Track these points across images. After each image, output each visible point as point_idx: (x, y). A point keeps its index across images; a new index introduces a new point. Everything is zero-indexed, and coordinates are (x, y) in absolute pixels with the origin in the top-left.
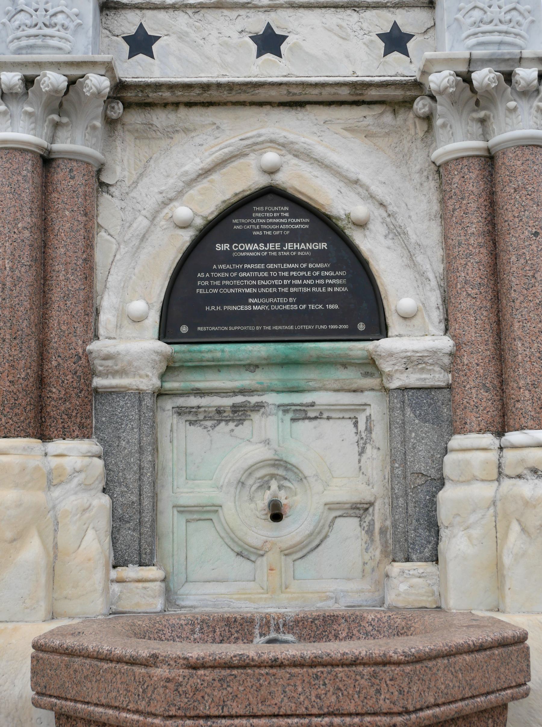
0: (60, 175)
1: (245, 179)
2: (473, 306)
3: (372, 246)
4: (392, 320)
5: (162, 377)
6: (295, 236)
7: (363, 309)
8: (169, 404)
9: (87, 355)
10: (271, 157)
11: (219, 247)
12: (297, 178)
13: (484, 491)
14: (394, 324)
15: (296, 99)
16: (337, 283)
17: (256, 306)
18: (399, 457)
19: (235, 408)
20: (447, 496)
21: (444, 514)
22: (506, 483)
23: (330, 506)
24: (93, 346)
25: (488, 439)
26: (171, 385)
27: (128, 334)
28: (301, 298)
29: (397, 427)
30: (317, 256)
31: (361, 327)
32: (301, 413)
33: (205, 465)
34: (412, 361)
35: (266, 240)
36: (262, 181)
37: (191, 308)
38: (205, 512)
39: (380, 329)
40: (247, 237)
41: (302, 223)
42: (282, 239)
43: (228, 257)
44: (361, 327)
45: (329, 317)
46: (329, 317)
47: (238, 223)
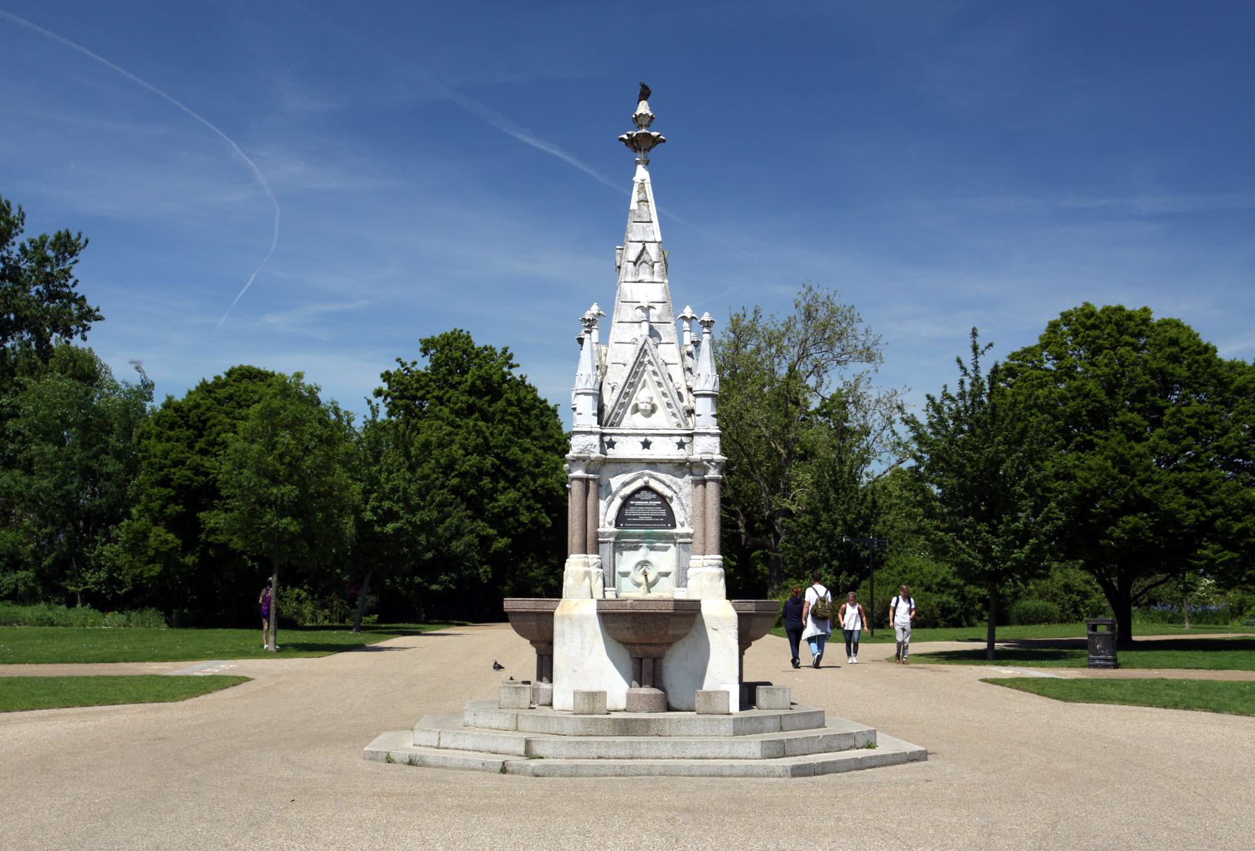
2: (698, 520)
6: (652, 500)
7: (670, 520)
10: (646, 478)
12: (654, 484)
14: (678, 525)
15: (652, 464)
16: (663, 513)
17: (642, 519)
18: (679, 560)
32: (652, 549)
33: (628, 561)
38: (625, 574)
39: (674, 526)
40: (639, 500)
41: (654, 496)
47: (637, 496)
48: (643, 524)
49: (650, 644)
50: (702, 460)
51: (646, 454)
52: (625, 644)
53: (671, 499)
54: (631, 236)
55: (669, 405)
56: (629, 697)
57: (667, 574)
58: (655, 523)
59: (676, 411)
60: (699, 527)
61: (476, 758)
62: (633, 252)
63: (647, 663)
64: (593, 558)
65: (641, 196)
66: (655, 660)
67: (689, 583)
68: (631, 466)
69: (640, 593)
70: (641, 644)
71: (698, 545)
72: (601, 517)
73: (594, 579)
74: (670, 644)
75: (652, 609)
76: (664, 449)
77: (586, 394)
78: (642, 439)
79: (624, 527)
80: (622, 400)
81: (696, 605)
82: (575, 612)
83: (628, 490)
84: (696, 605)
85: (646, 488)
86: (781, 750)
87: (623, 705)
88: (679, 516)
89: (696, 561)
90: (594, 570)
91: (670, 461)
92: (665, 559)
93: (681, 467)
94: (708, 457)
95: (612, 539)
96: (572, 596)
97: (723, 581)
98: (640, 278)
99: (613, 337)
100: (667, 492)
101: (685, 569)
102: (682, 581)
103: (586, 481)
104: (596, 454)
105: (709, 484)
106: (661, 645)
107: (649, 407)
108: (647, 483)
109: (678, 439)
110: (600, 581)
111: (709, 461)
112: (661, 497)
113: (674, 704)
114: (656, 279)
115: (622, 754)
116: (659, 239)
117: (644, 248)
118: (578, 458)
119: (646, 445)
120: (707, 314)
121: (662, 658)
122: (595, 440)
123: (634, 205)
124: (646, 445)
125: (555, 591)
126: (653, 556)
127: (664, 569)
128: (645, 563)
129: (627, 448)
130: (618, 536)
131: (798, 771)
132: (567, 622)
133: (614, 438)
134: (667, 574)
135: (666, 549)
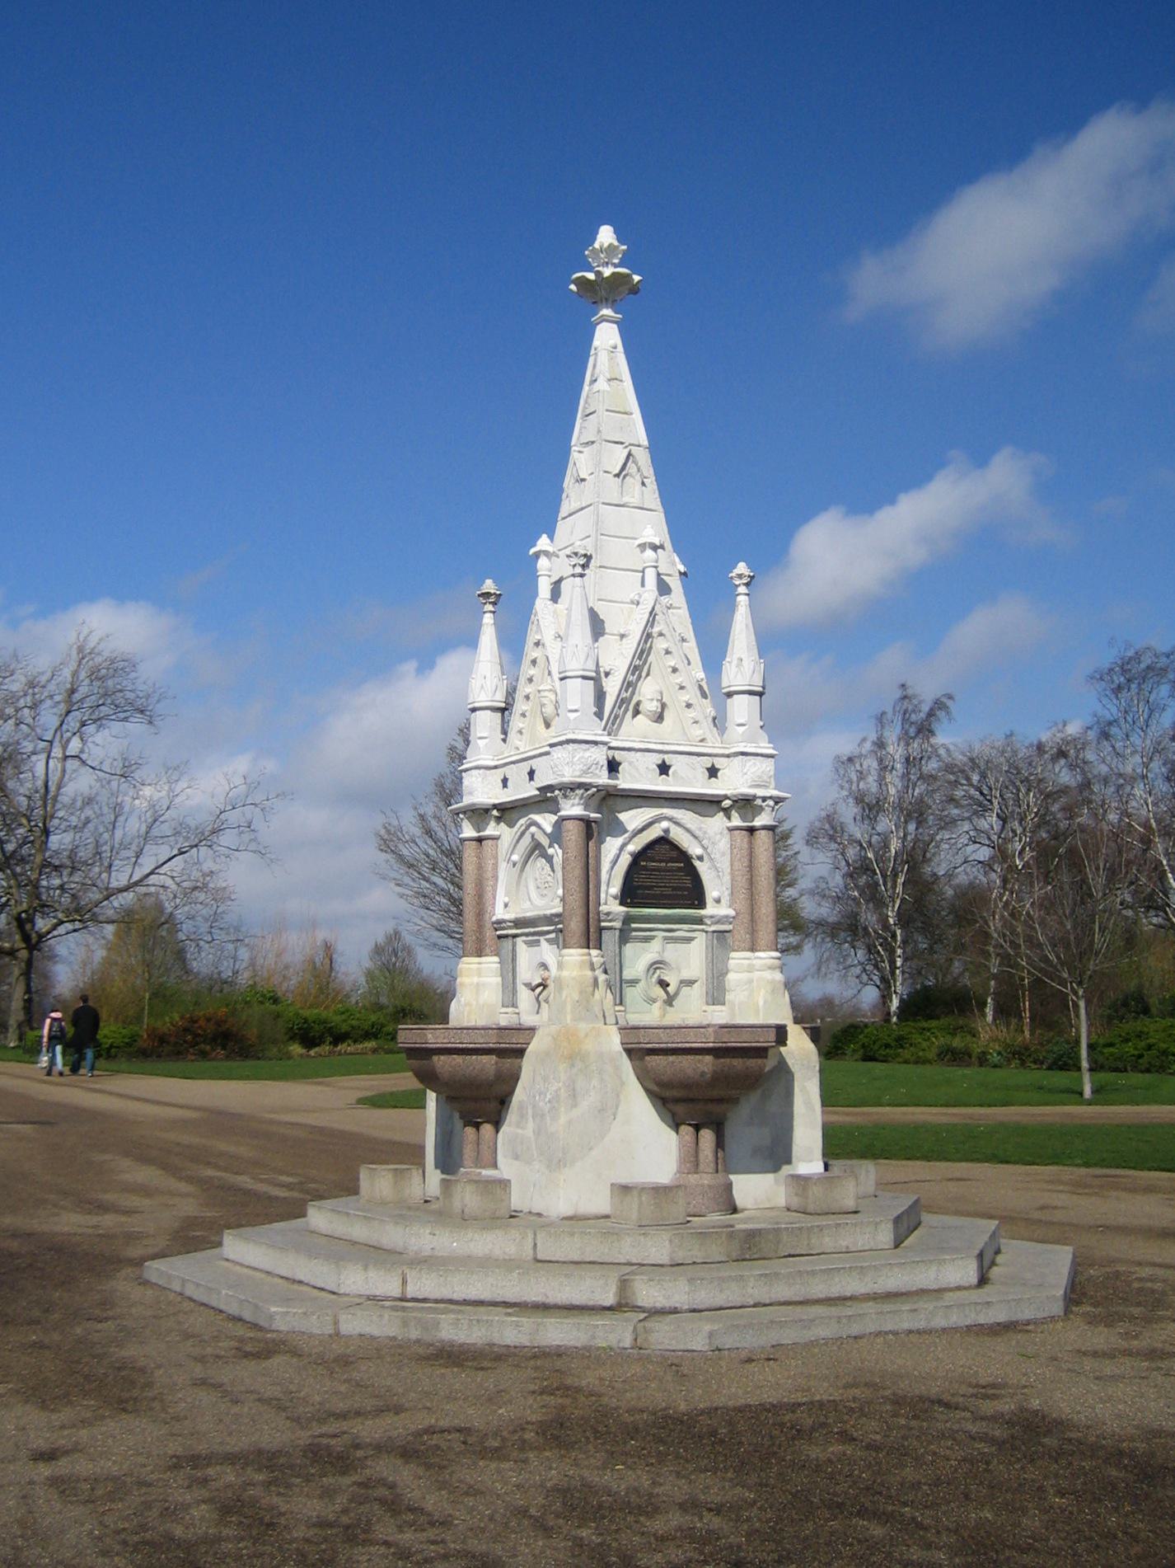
1: (654, 833)
2: (742, 895)
3: (702, 868)
6: (672, 860)
7: (695, 895)
10: (665, 824)
12: (677, 835)
13: (745, 976)
16: (688, 882)
17: (658, 891)
20: (731, 976)
23: (682, 982)
25: (748, 954)
27: (610, 904)
28: (674, 889)
29: (710, 948)
34: (720, 920)
35: (661, 861)
37: (630, 894)
39: (702, 904)
41: (674, 854)
43: (645, 868)
45: (683, 897)
46: (683, 897)
53: (700, 858)
57: (690, 983)
59: (700, 718)
60: (742, 905)
71: (741, 934)
72: (603, 887)
76: (688, 779)
77: (584, 678)
80: (624, 695)
88: (711, 893)
89: (738, 959)
93: (706, 804)
95: (618, 924)
98: (626, 499)
100: (694, 850)
101: (724, 973)
102: (716, 995)
103: (587, 823)
104: (603, 778)
105: (762, 835)
108: (667, 831)
109: (708, 762)
116: (646, 443)
126: (672, 953)
127: (686, 974)
128: (656, 965)
129: (637, 776)
130: (628, 919)
134: (690, 983)
135: (689, 940)
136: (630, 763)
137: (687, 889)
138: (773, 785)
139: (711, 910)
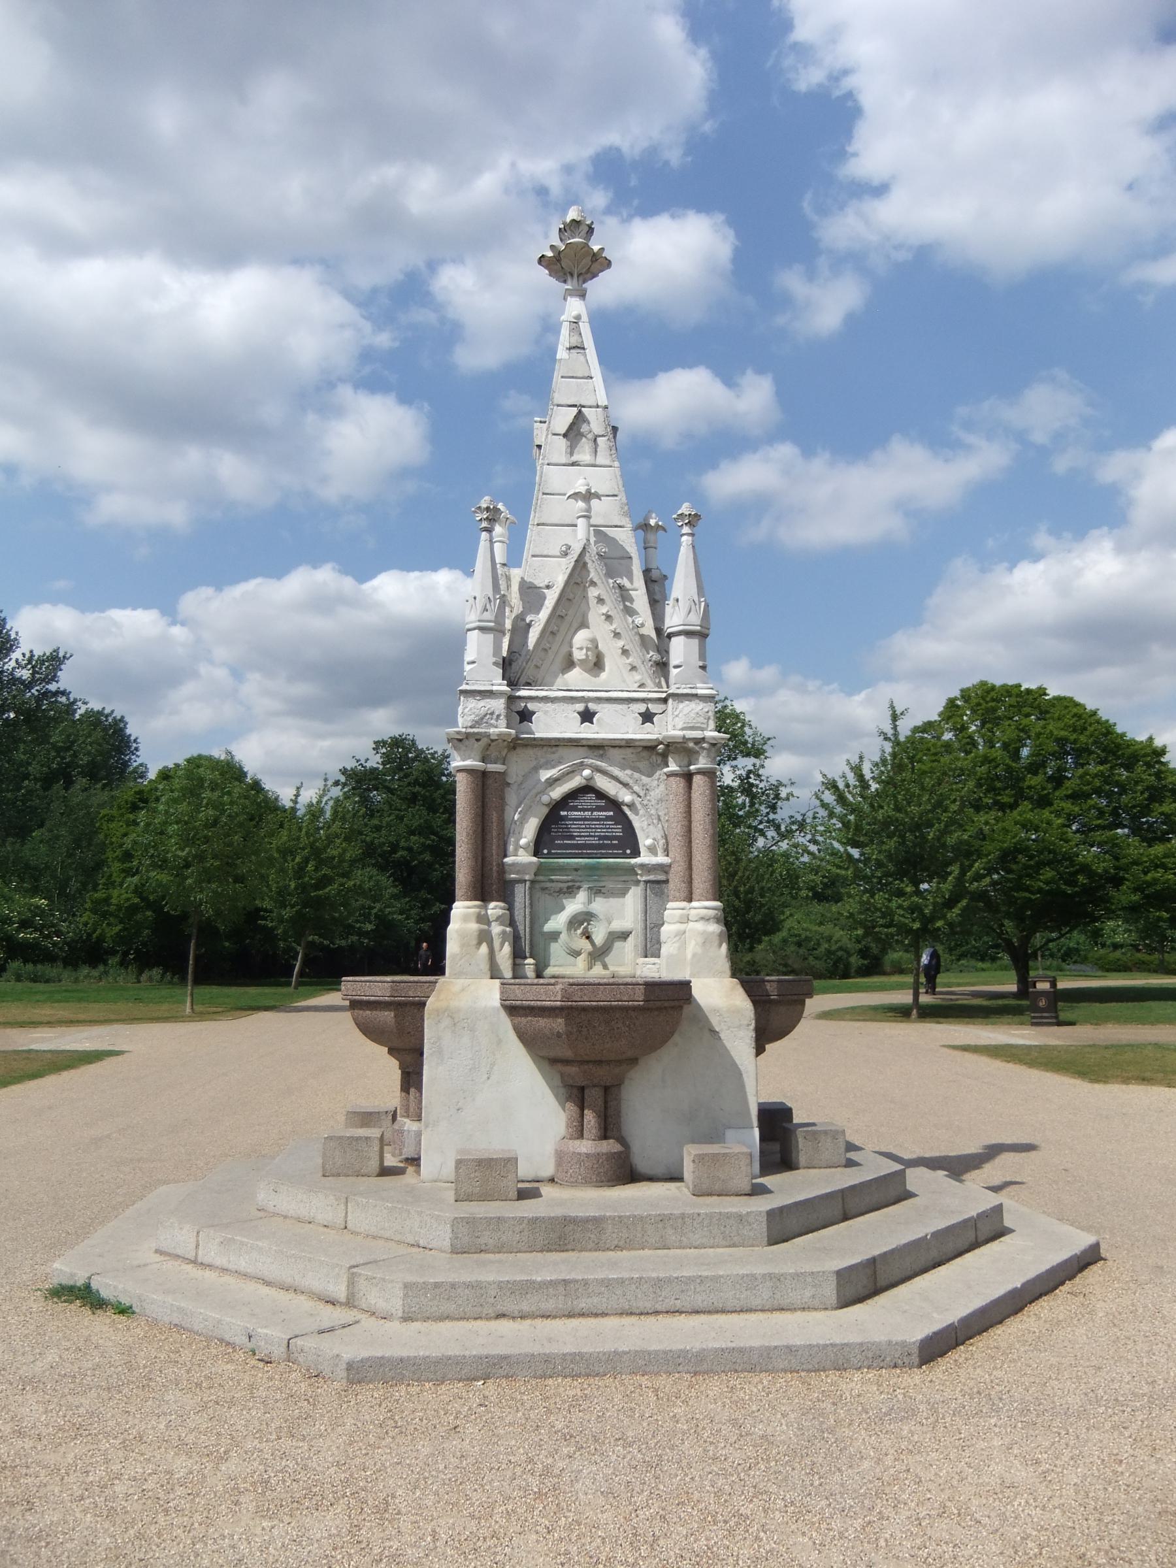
0: (490, 781)
2: (676, 844)
4: (642, 849)
5: (535, 875)
6: (599, 809)
7: (629, 843)
8: (537, 886)
9: (503, 864)
10: (587, 772)
11: (562, 813)
12: (602, 783)
15: (598, 748)
16: (618, 831)
19: (568, 888)
20: (665, 929)
21: (663, 938)
22: (691, 924)
23: (611, 933)
24: (506, 860)
25: (684, 904)
26: (540, 878)
28: (600, 838)
30: (608, 818)
31: (628, 851)
35: (584, 810)
36: (584, 782)
39: (636, 853)
40: (575, 809)
41: (602, 803)
42: (592, 810)
44: (628, 851)
48: (582, 850)
49: (599, 1062)
50: (686, 740)
51: (588, 732)
52: (554, 1061)
53: (631, 806)
54: (558, 397)
55: (625, 652)
56: (560, 1156)
57: (624, 936)
58: (602, 847)
59: (638, 663)
61: (234, 1326)
62: (563, 419)
63: (593, 1095)
64: (495, 909)
65: (575, 341)
66: (606, 1089)
67: (664, 950)
68: (562, 751)
69: (578, 969)
70: (582, 1062)
71: (676, 882)
73: (497, 943)
74: (634, 1061)
75: (603, 999)
78: (580, 707)
79: (550, 855)
81: (682, 990)
82: (462, 1002)
83: (557, 793)
84: (682, 990)
85: (587, 789)
86: (866, 1282)
87: (548, 1170)
88: (644, 842)
90: (496, 929)
91: (628, 744)
92: (623, 911)
94: (697, 734)
96: (458, 975)
97: (724, 946)
99: (530, 548)
102: (651, 947)
104: (500, 728)
106: (619, 1062)
107: (592, 658)
109: (642, 708)
110: (507, 949)
111: (698, 741)
112: (614, 804)
113: (641, 1163)
114: (600, 460)
115: (549, 1305)
117: (580, 411)
118: (468, 736)
119: (587, 716)
120: (686, 505)
121: (619, 1085)
122: (499, 705)
123: (562, 353)
124: (587, 716)
125: (437, 967)
126: (599, 905)
127: (617, 925)
129: (554, 722)
130: (540, 870)
131: (936, 1348)
132: (446, 1022)
133: (531, 706)
134: (624, 936)
136: (546, 713)
137: (615, 838)
138: (712, 725)
139: (645, 858)
